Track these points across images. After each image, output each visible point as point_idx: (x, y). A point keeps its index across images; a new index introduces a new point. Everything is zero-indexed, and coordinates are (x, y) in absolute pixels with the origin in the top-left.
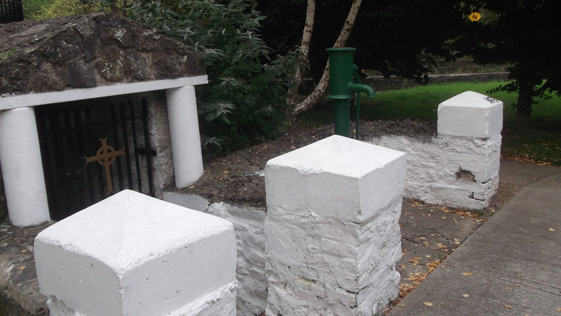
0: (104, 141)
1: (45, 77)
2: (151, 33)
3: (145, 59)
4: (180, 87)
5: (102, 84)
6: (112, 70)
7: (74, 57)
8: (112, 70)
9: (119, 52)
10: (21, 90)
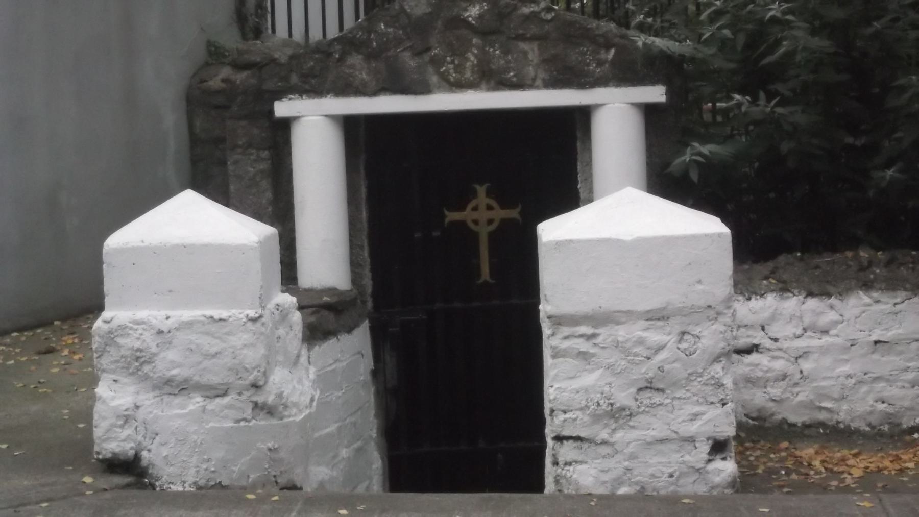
0: (481, 190)
3: (525, 53)
4: (604, 104)
5: (440, 89)
6: (459, 69)
8: (459, 69)
9: (471, 40)
10: (317, 92)
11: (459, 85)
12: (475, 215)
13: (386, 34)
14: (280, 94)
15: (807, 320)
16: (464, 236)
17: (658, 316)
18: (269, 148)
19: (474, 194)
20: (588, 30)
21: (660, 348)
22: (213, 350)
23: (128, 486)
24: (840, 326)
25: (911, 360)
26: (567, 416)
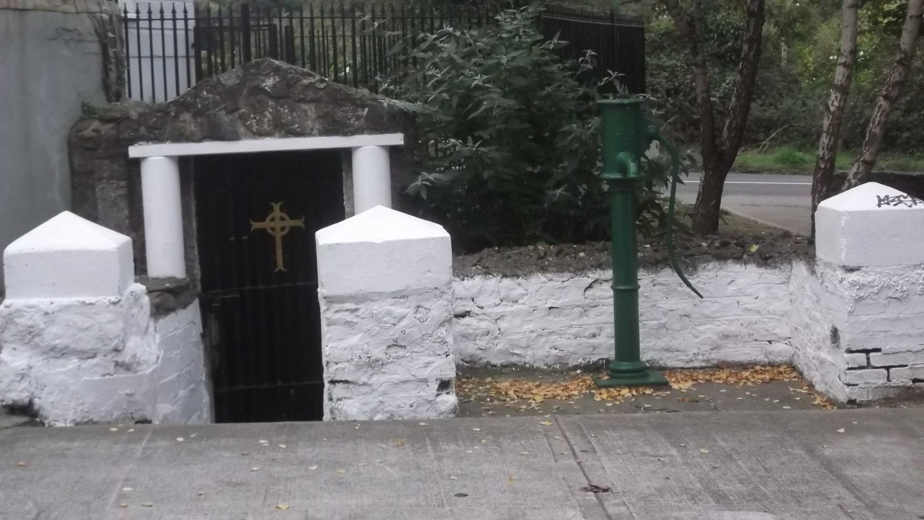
0: (277, 207)
1: (183, 127)
2: (313, 80)
3: (306, 111)
5: (246, 137)
6: (260, 122)
7: (214, 108)
9: (267, 103)
11: (260, 134)
12: (272, 224)
13: (207, 99)
14: (133, 141)
15: (503, 294)
17: (400, 296)
18: (125, 179)
19: (271, 209)
21: (403, 318)
22: (86, 325)
23: (24, 424)
24: (525, 297)
25: (574, 320)
26: (338, 366)
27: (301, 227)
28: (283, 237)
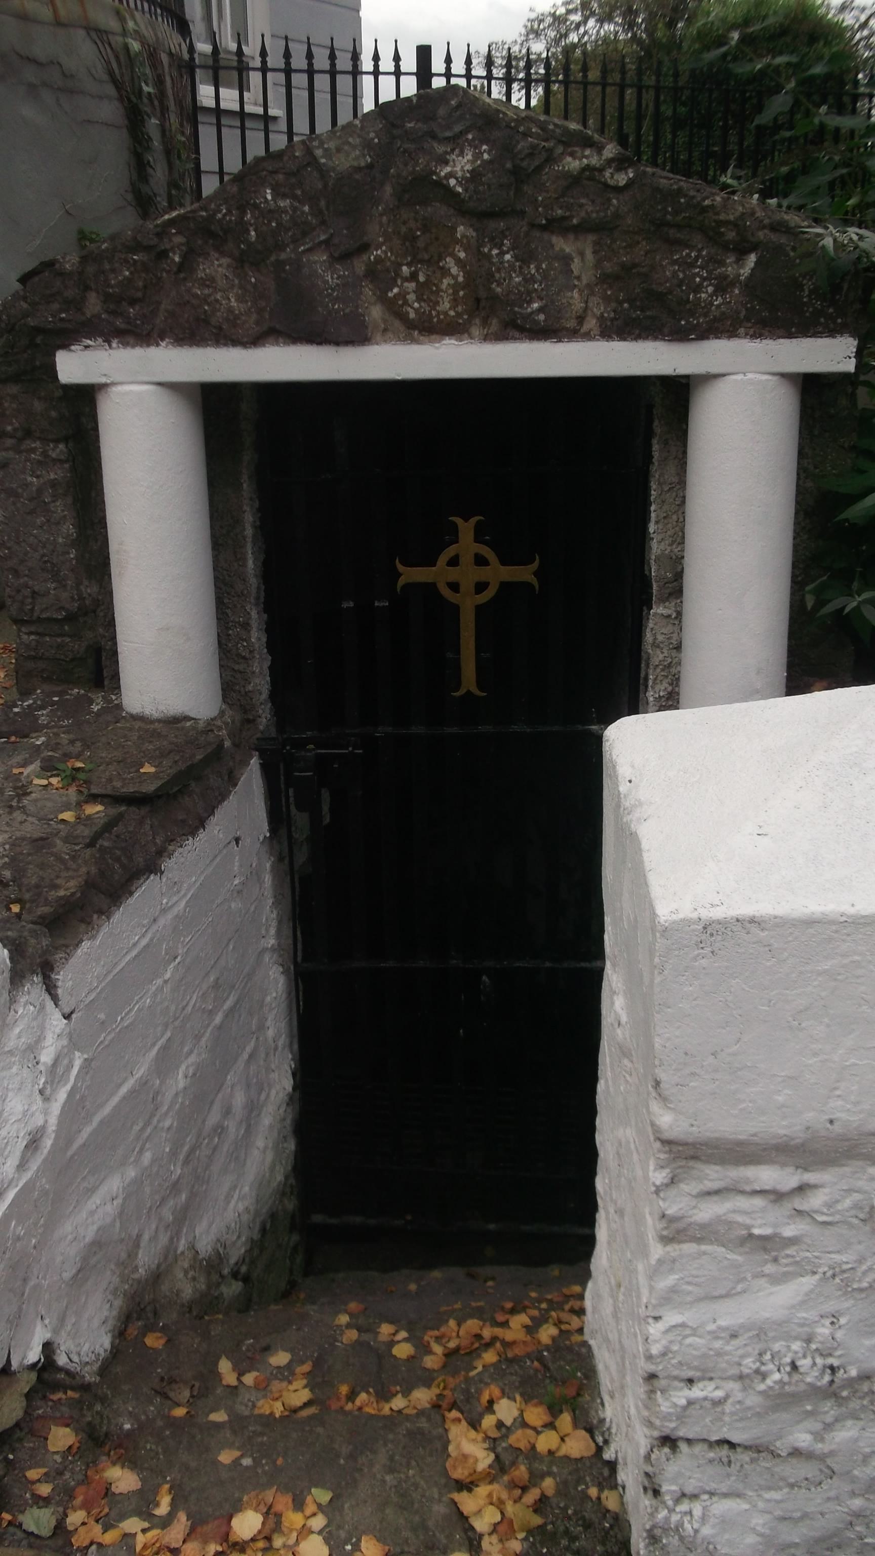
0: (466, 528)
1: (205, 300)
2: (594, 161)
3: (566, 260)
4: (724, 375)
5: (387, 334)
6: (427, 291)
7: (295, 241)
8: (427, 291)
9: (454, 229)
10: (138, 333)
12: (453, 574)
13: (273, 213)
14: (67, 337)
16: (435, 608)
18: (66, 440)
20: (704, 210)
26: (696, 1392)
27: (529, 585)
28: (480, 610)
